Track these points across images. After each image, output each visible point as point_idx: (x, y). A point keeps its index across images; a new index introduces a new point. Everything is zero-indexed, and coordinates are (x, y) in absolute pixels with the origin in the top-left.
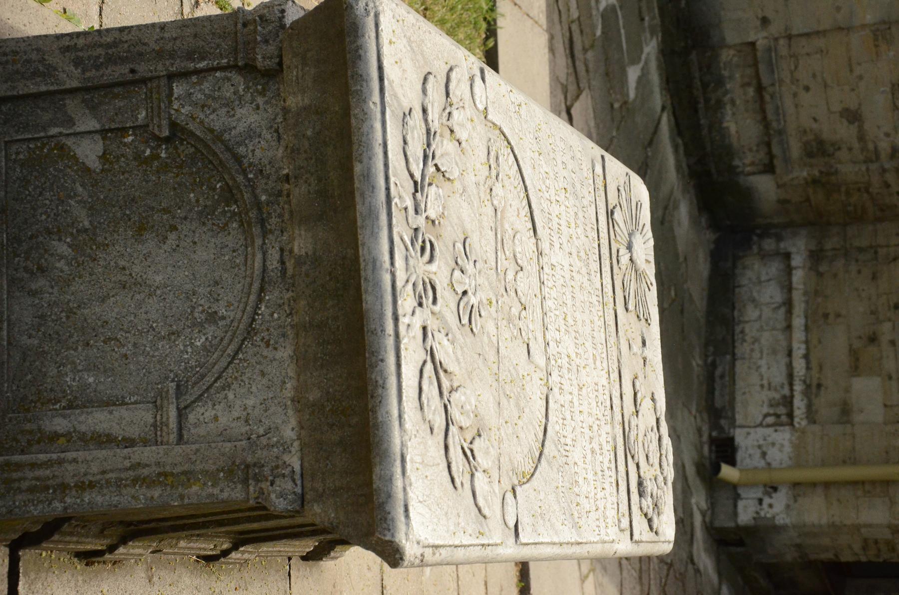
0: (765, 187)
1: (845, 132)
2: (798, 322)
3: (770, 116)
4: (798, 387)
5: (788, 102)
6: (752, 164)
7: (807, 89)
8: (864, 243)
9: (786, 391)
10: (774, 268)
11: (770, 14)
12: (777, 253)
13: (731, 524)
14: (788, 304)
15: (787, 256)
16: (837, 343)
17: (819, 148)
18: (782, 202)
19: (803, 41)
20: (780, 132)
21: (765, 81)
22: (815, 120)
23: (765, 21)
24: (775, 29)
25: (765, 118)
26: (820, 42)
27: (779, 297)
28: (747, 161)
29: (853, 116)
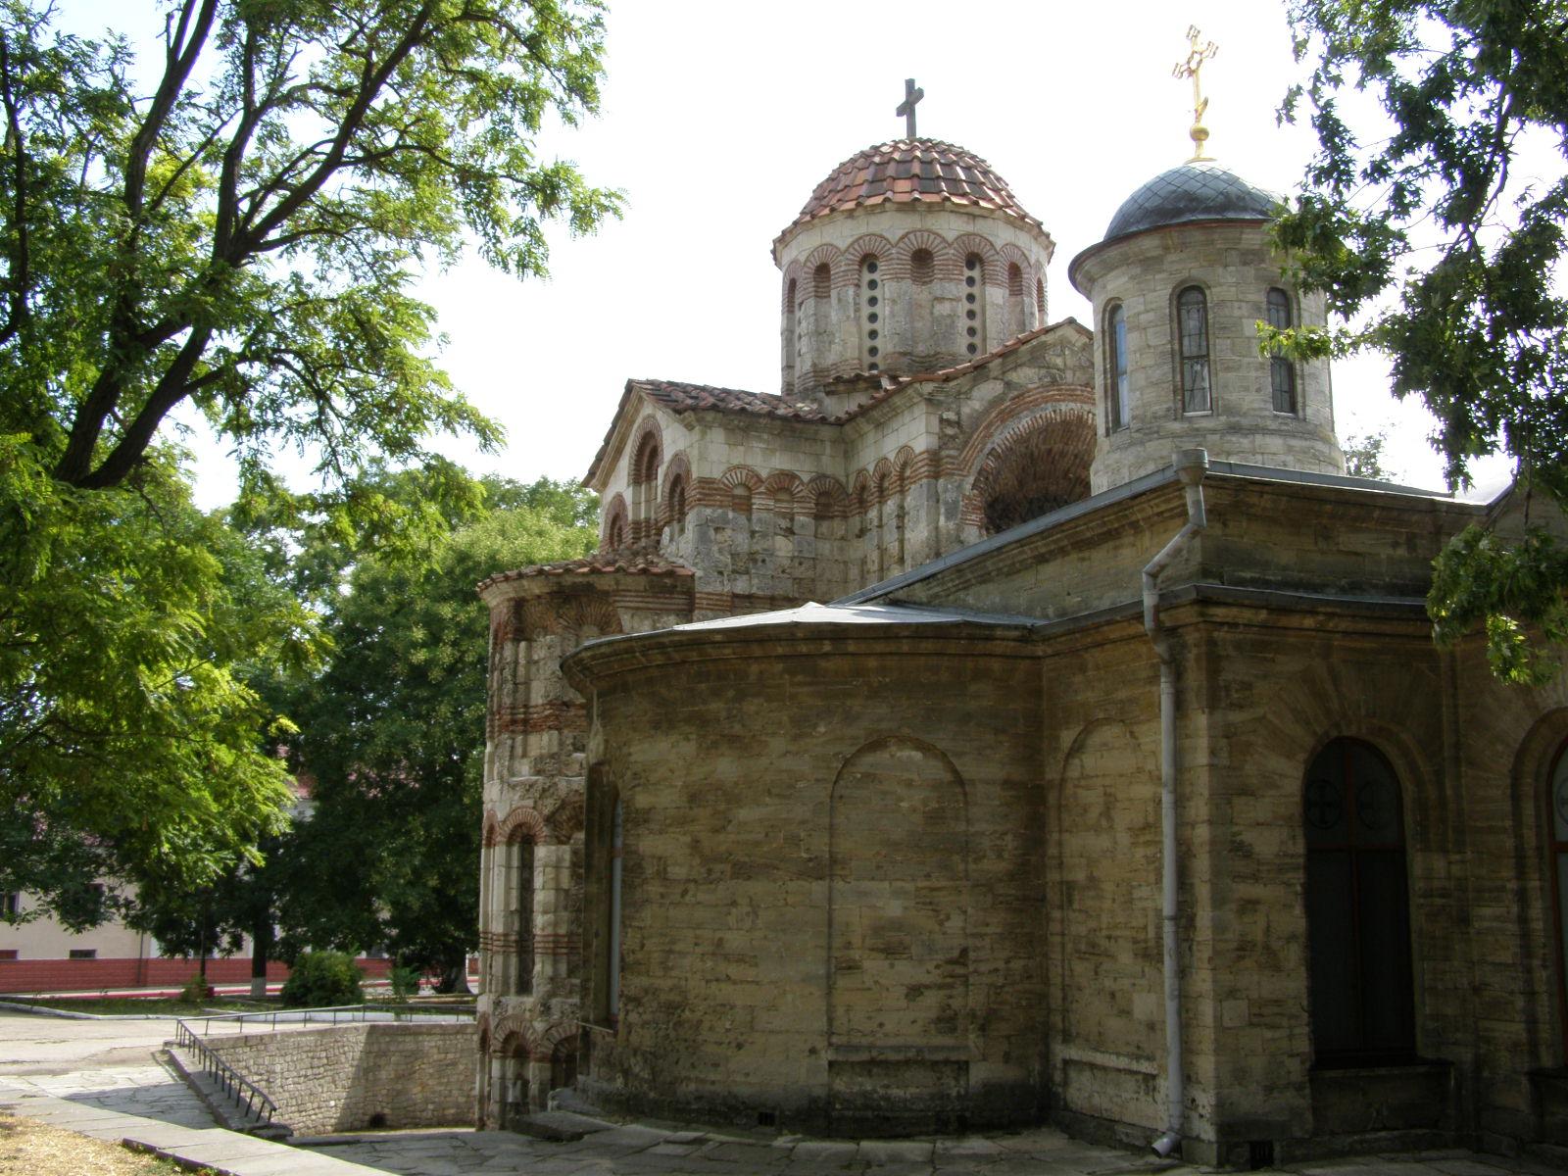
0: (980, 1074)
1: (931, 1000)
2: (1099, 1058)
3: (900, 1057)
4: (1135, 1066)
5: (893, 1041)
6: (957, 1079)
7: (881, 1025)
8: (1059, 994)
9: (1140, 1077)
10: (1073, 1074)
11: (808, 1046)
12: (1065, 1071)
13: (1215, 1146)
14: (1092, 1066)
15: (1067, 1063)
16: (1114, 1024)
17: (947, 1021)
18: (1007, 1058)
19: (836, 1023)
20: (920, 1050)
21: (864, 1056)
22: (913, 1022)
23: (813, 1051)
24: (821, 1044)
25: (898, 1063)
26: (840, 1011)
27: (1087, 1074)
28: (953, 1083)
29: (915, 991)
